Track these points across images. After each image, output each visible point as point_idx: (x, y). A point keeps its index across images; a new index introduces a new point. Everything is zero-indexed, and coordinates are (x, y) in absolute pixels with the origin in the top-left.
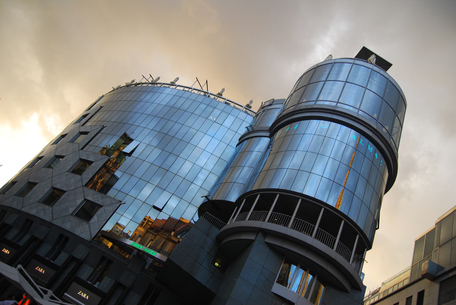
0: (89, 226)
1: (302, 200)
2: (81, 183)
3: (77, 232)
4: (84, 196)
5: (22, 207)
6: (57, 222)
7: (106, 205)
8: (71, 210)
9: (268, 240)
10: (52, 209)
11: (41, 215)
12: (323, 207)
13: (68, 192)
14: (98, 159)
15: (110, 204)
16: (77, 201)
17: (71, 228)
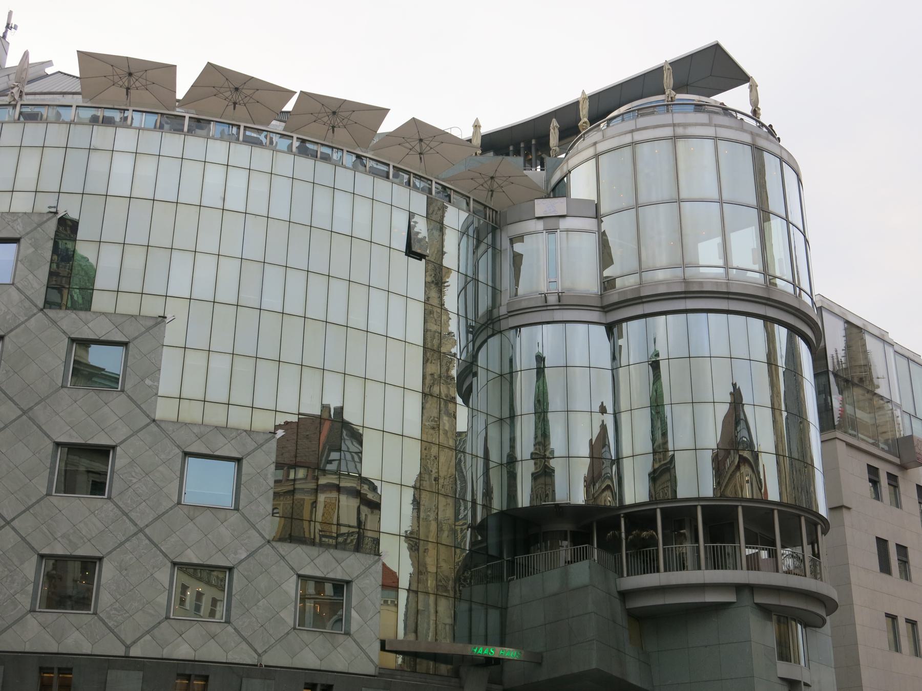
0: (355, 641)
1: (779, 511)
2: (253, 532)
3: (340, 666)
4: (292, 569)
5: (128, 647)
6: (277, 658)
7: (357, 577)
8: (289, 616)
9: (760, 599)
10: (235, 629)
11: (213, 652)
12: (802, 515)
13: (240, 568)
14: (250, 448)
15: (364, 572)
16: (284, 586)
17: (321, 661)
